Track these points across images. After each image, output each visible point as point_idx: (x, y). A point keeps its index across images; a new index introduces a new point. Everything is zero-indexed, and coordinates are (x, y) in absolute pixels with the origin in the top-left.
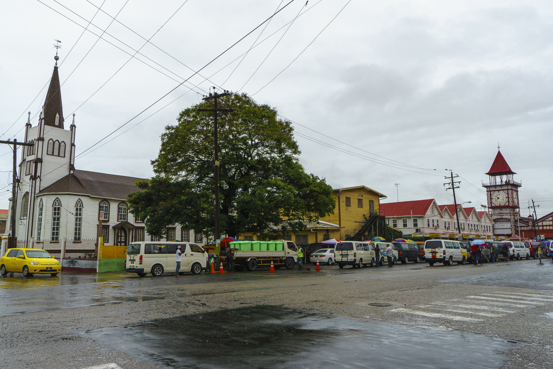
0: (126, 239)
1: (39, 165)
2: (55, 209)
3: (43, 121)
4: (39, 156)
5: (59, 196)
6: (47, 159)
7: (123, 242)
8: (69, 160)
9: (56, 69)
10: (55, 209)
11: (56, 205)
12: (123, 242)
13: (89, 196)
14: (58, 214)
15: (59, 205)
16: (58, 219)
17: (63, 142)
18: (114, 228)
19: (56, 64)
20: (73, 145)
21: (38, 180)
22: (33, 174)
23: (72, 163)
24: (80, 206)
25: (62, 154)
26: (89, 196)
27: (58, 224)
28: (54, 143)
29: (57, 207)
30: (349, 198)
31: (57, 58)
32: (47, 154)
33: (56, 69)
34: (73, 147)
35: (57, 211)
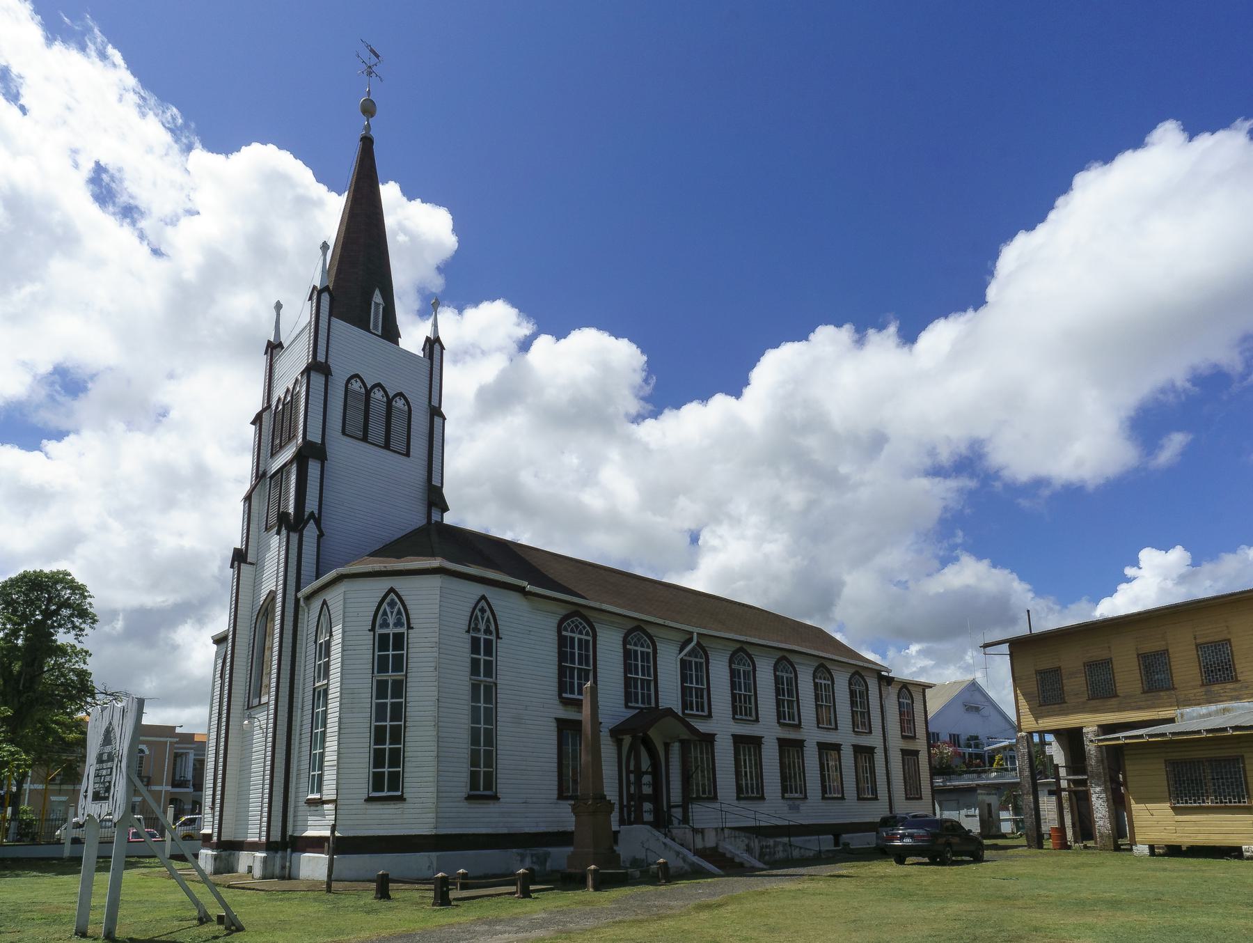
0: (656, 785)
1: (313, 468)
2: (383, 642)
3: (326, 298)
4: (315, 437)
5: (400, 584)
6: (343, 450)
7: (647, 798)
8: (421, 473)
9: (367, 142)
10: (383, 639)
11: (385, 624)
12: (647, 798)
13: (521, 590)
14: (399, 664)
15: (398, 623)
16: (399, 688)
17: (401, 395)
18: (616, 733)
19: (368, 127)
20: (436, 413)
21: (311, 531)
22: (291, 510)
23: (436, 482)
24: (487, 631)
25: (397, 441)
26: (521, 590)
27: (398, 711)
28: (368, 392)
29: (391, 630)
30: (1107, 664)
31: (368, 109)
32: (344, 433)
33: (367, 142)
34: (437, 420)
35: (390, 649)
